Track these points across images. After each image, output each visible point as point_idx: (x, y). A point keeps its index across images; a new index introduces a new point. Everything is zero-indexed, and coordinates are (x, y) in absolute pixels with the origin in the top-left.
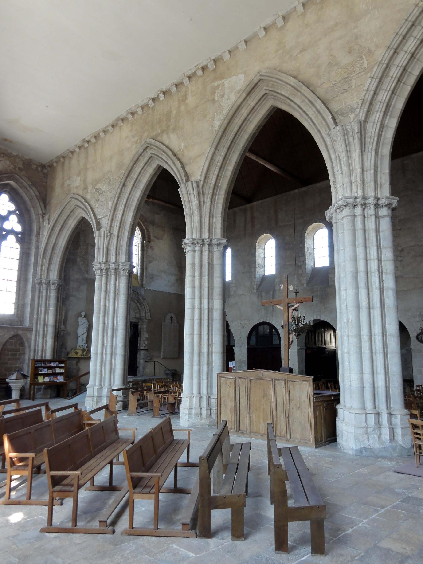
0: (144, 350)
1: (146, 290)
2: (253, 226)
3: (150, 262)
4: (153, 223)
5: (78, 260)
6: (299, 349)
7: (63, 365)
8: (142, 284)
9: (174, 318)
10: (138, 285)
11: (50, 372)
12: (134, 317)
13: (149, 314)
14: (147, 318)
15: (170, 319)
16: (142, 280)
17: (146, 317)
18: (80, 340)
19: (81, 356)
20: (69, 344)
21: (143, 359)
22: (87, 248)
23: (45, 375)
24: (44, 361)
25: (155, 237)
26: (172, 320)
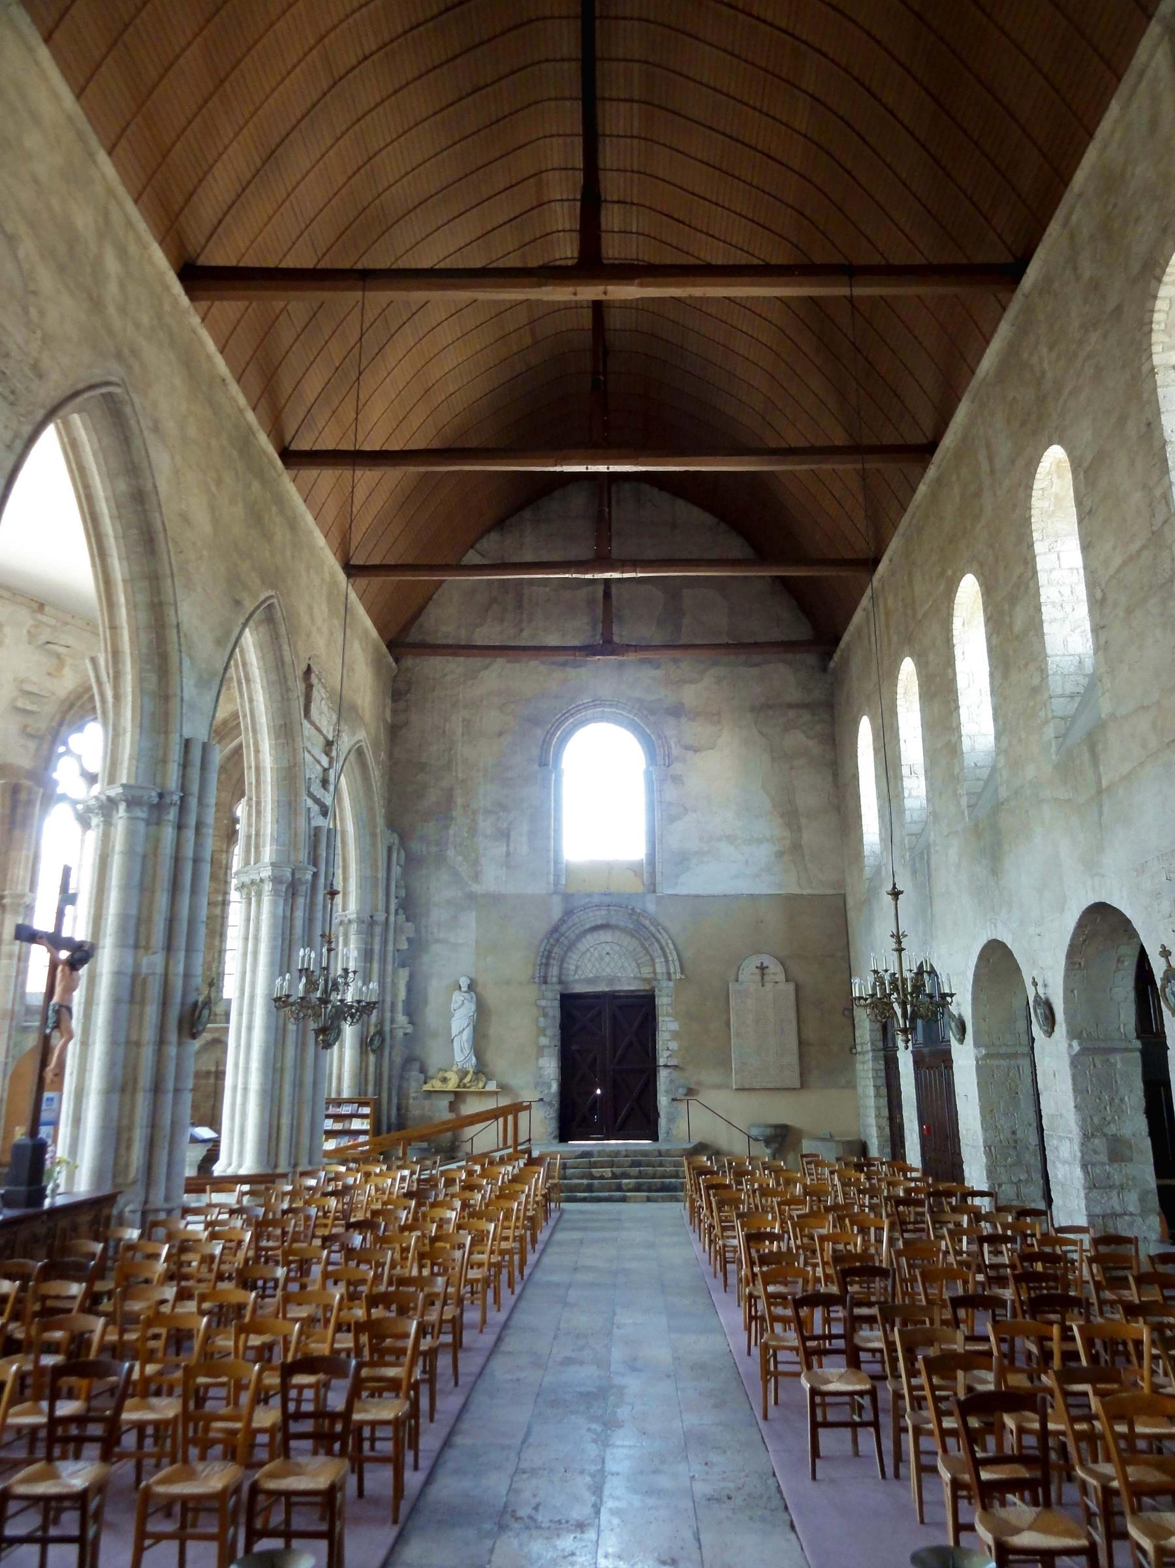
0: (666, 1066)
1: (660, 900)
2: (889, 644)
3: (672, 819)
4: (677, 711)
5: (451, 853)
6: (988, 1056)
7: (366, 1110)
8: (654, 885)
9: (775, 969)
10: (641, 889)
11: (338, 1126)
12: (635, 978)
13: (677, 963)
14: (673, 977)
15: (757, 971)
16: (653, 874)
17: (669, 974)
18: (456, 1045)
19: (459, 1086)
20: (413, 1061)
21: (666, 1092)
22: (474, 820)
23: (331, 1134)
24: (339, 1103)
25: (688, 748)
26: (763, 975)
